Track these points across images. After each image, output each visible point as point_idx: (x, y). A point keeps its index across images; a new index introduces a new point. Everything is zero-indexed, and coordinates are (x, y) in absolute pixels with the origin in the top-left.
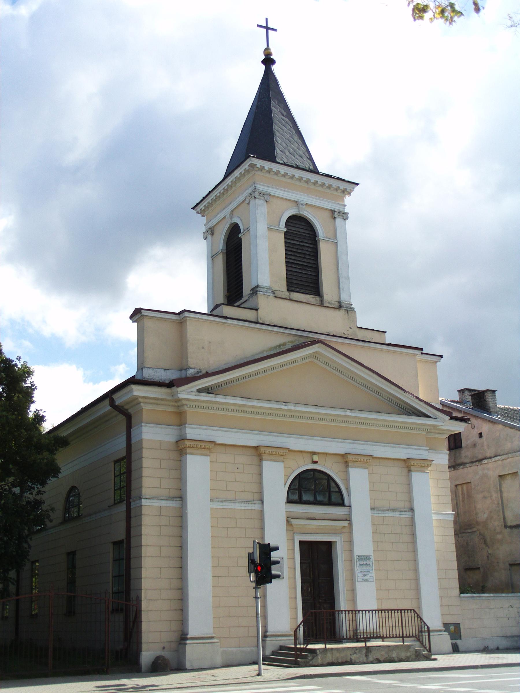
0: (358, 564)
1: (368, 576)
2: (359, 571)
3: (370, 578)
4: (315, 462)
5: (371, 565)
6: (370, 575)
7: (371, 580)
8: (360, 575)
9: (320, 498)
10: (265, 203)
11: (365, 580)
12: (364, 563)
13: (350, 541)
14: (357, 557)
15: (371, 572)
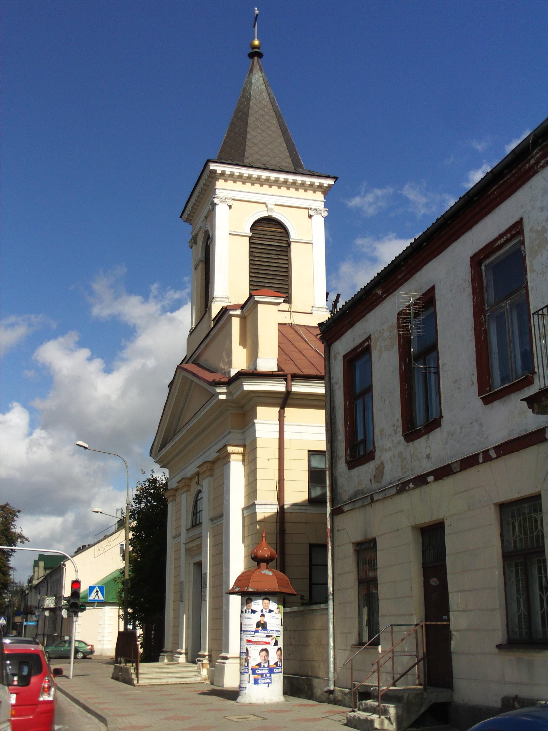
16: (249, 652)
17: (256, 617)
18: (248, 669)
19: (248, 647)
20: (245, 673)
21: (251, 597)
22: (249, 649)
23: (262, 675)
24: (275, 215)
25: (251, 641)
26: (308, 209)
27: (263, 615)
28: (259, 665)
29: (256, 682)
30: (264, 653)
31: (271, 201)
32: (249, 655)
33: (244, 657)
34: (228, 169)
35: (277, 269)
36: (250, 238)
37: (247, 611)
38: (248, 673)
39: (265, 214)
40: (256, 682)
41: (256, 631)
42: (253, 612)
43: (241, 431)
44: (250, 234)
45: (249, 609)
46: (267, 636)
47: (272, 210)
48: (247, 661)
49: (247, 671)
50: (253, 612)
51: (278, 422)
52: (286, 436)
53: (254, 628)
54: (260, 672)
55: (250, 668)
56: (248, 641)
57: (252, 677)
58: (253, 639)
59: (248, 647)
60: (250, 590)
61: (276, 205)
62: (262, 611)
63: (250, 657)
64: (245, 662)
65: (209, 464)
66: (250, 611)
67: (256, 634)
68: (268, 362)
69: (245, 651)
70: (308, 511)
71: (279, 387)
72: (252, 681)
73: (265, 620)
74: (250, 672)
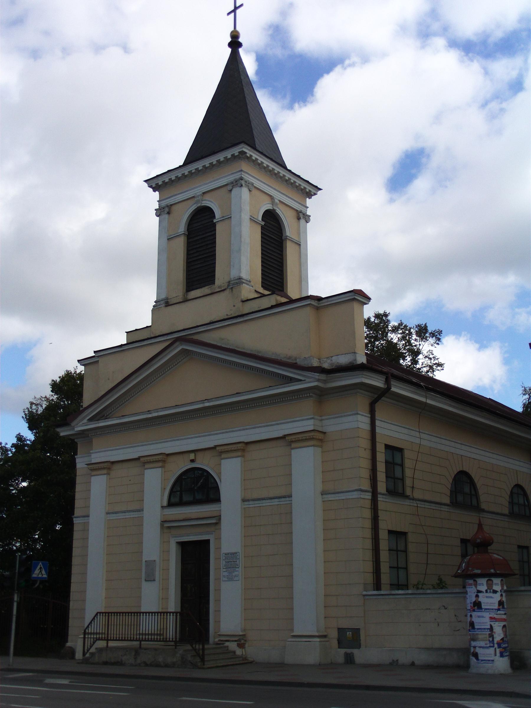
0: (224, 562)
1: (234, 574)
2: (225, 570)
3: (236, 576)
4: (192, 461)
5: (238, 562)
6: (236, 573)
7: (236, 579)
8: (226, 574)
9: (198, 496)
10: (167, 216)
11: (230, 579)
12: (231, 560)
13: (219, 538)
14: (224, 555)
15: (237, 569)
16: (494, 628)
17: (497, 597)
18: (493, 643)
19: (492, 623)
20: (490, 647)
21: (493, 579)
22: (493, 625)
23: (505, 648)
24: (278, 211)
25: (494, 618)
26: (297, 211)
27: (501, 595)
28: (502, 639)
29: (502, 655)
30: (504, 629)
31: (278, 196)
32: (494, 630)
33: (488, 633)
34: (255, 155)
35: (276, 263)
36: (262, 228)
37: (489, 591)
38: (493, 646)
39: (269, 207)
40: (502, 655)
41: (499, 610)
42: (495, 592)
43: (320, 418)
44: (263, 223)
45: (490, 590)
46: (505, 614)
47: (277, 204)
48: (491, 636)
49: (492, 645)
50: (495, 592)
51: (369, 416)
52: (378, 430)
53: (496, 606)
54: (504, 646)
55: (495, 642)
56: (491, 618)
57: (498, 651)
58: (495, 616)
59: (492, 623)
60: (498, 572)
61: (280, 201)
62: (501, 591)
63: (495, 633)
64: (490, 637)
65: (243, 445)
66: (492, 591)
67: (499, 612)
68: (362, 359)
69: (489, 627)
70: (387, 500)
71: (378, 382)
72: (498, 654)
73: (480, 599)
74: (496, 646)
